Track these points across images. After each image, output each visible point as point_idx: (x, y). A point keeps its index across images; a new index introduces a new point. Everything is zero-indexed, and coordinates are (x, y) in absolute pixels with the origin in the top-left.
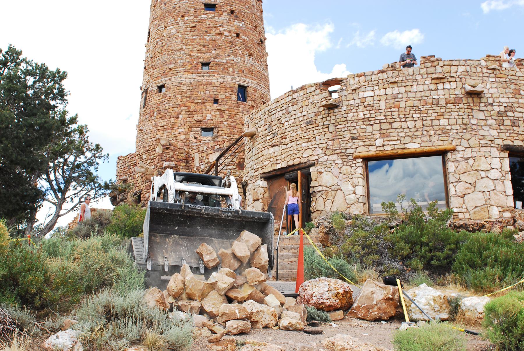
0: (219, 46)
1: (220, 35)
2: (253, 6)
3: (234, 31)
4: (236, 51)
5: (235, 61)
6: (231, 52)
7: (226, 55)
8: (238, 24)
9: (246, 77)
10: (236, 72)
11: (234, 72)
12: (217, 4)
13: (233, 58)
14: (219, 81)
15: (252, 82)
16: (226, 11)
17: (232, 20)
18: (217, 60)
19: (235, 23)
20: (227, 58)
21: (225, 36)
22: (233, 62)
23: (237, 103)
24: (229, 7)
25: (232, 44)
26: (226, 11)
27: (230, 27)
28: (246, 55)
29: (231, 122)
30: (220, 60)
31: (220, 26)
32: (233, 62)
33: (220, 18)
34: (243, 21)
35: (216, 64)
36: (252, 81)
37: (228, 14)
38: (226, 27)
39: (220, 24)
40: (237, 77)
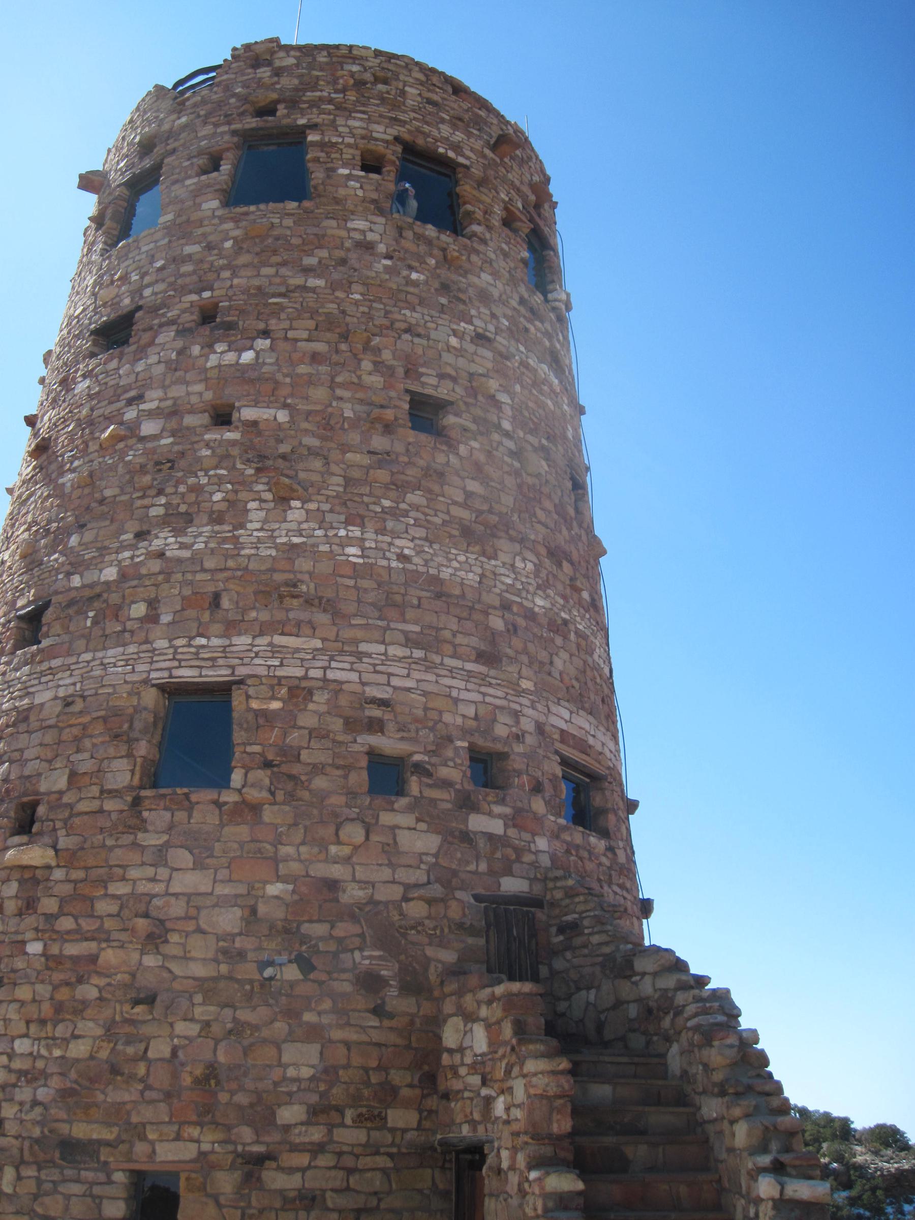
0: (102, 502)
1: (121, 445)
2: (367, 247)
3: (194, 399)
4: (192, 497)
5: (168, 554)
6: (161, 511)
7: (128, 537)
8: (230, 357)
9: (231, 628)
10: (165, 619)
11: (152, 618)
12: (139, 308)
13: (164, 540)
14: (61, 693)
15: (275, 650)
16: (172, 322)
17: (196, 350)
18: (76, 581)
19: (213, 360)
20: (127, 554)
21: (143, 439)
22: (155, 566)
23: (137, 802)
24: (194, 297)
25: (171, 468)
26: (172, 322)
27: (177, 391)
28: (252, 505)
29: (64, 937)
30: (91, 576)
31: (130, 402)
32: (155, 566)
33: (140, 367)
34: (265, 334)
35: (71, 603)
36: (279, 640)
37: (181, 333)
38: (159, 393)
39: (132, 393)
40: (161, 644)
